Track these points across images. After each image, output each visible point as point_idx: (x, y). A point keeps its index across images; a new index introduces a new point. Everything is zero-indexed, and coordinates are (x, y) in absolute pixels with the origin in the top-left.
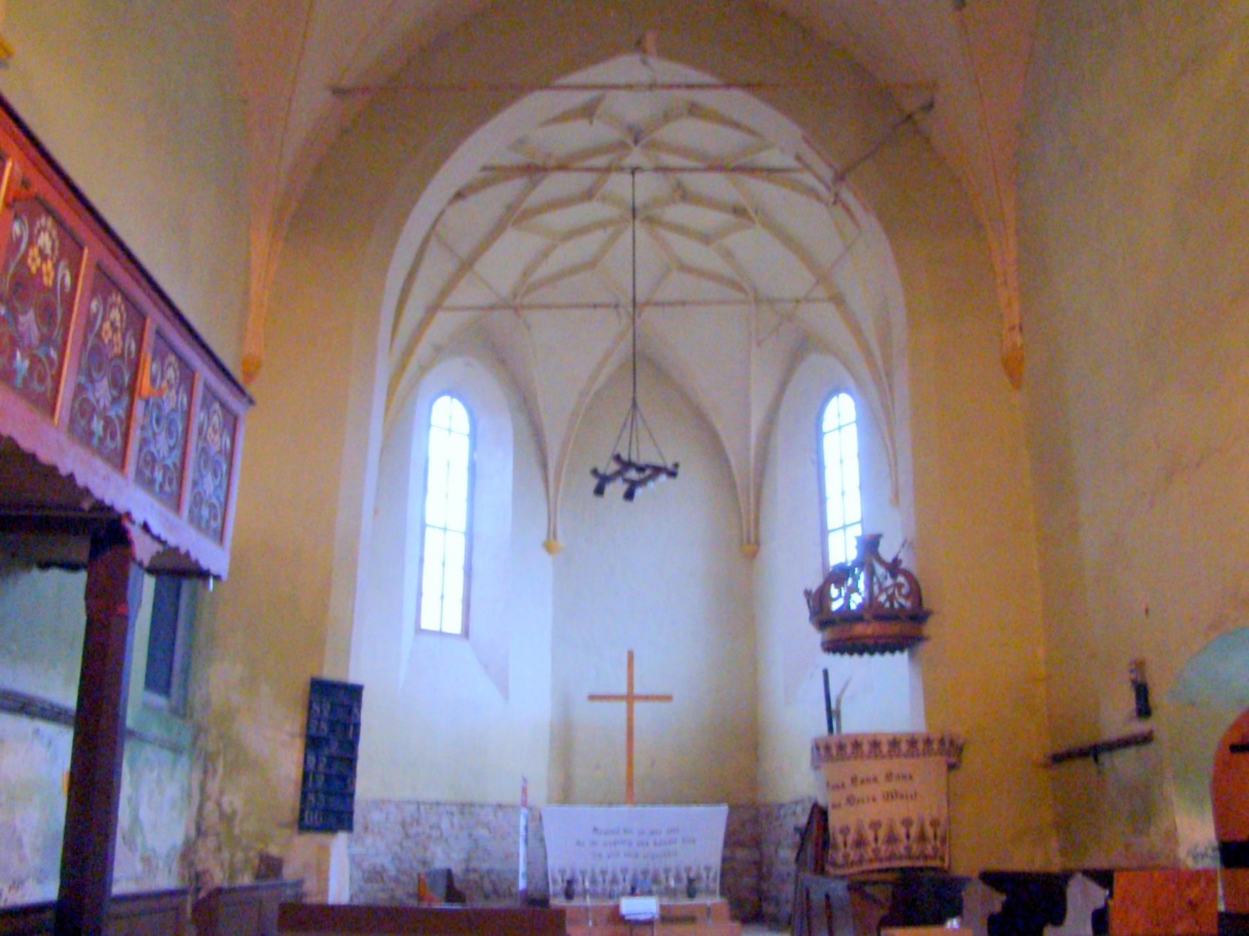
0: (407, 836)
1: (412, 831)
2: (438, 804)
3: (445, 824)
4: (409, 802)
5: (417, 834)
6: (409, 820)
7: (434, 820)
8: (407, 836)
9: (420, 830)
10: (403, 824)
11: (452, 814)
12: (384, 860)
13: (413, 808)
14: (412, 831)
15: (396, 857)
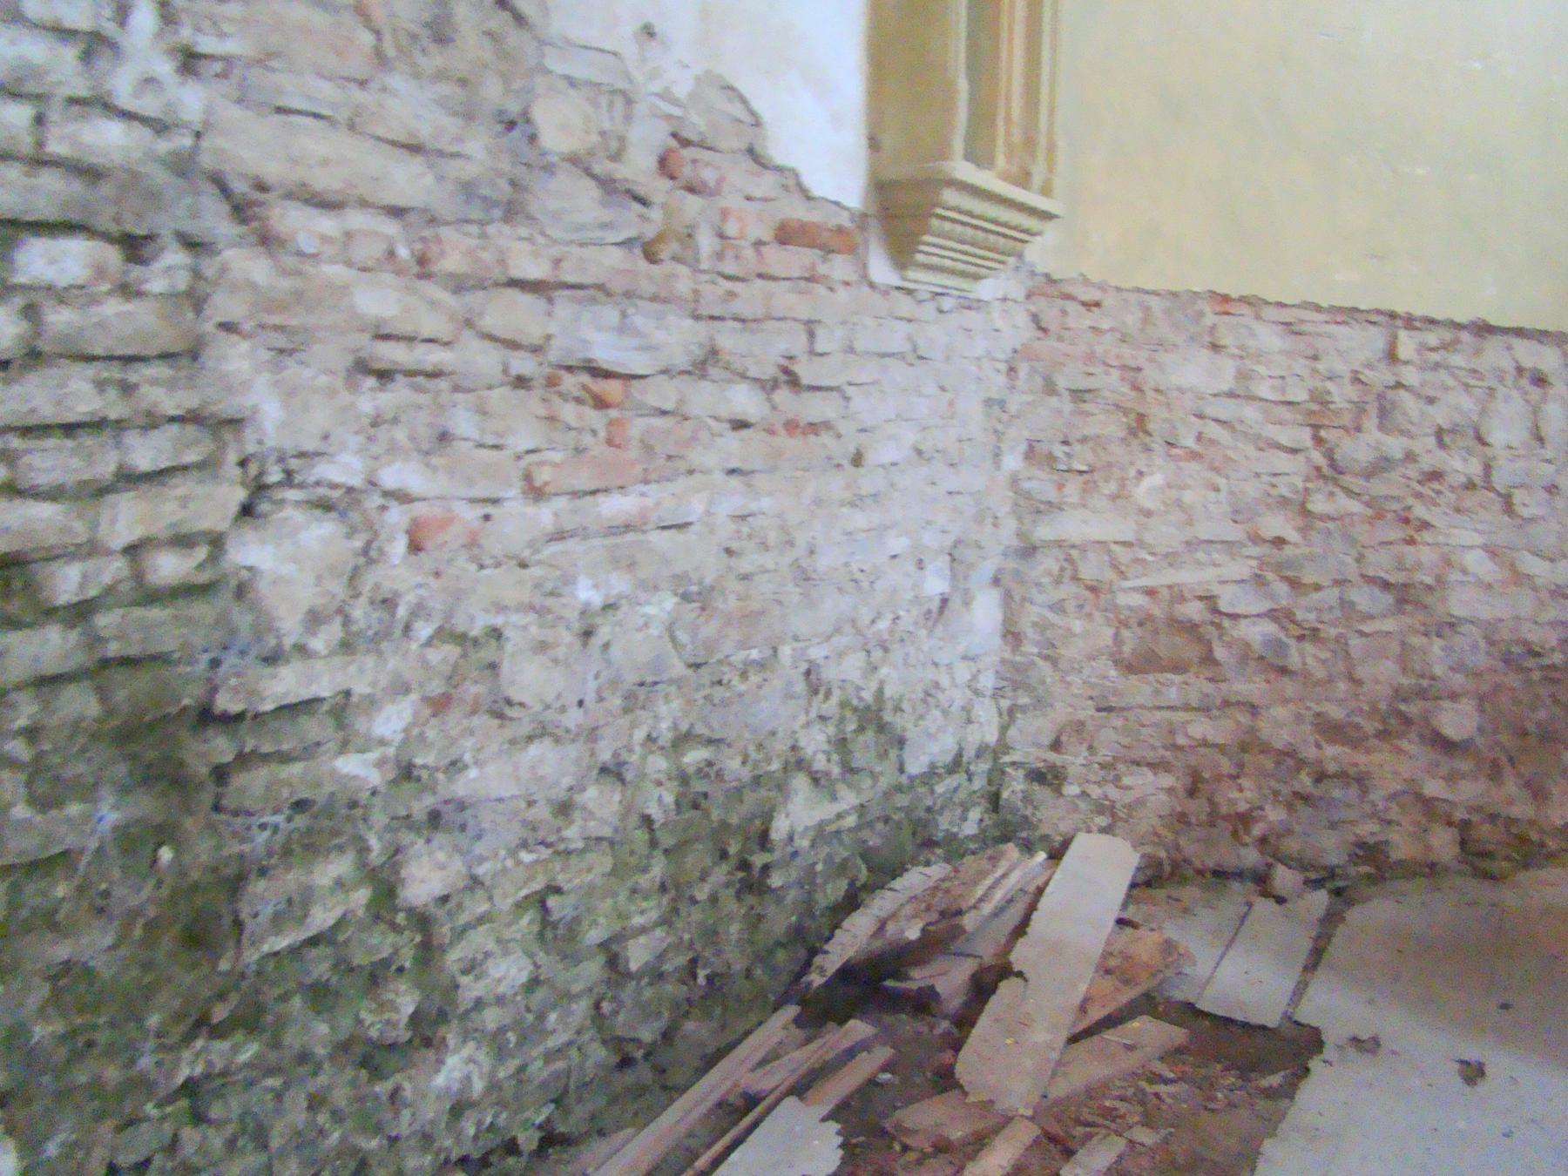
0: (1333, 472)
1: (1357, 450)
2: (1483, 329)
3: (1506, 431)
4: (1350, 314)
5: (1382, 465)
6: (1342, 395)
7: (1457, 405)
8: (1333, 472)
9: (1395, 446)
10: (1317, 414)
11: (1540, 380)
12: (1225, 577)
13: (1364, 344)
14: (1357, 450)
15: (1277, 567)
